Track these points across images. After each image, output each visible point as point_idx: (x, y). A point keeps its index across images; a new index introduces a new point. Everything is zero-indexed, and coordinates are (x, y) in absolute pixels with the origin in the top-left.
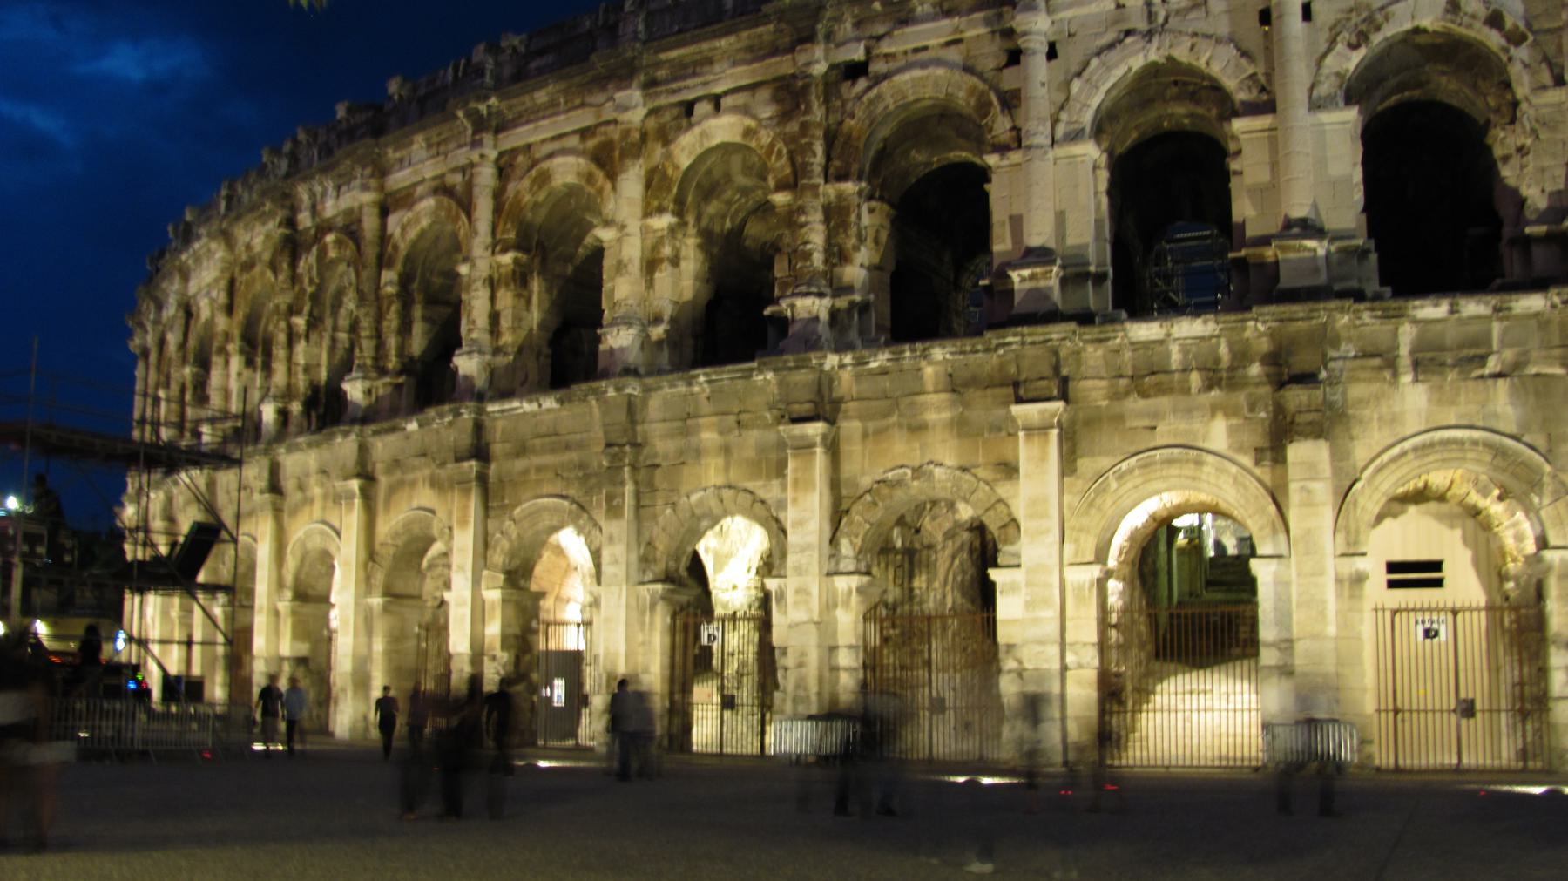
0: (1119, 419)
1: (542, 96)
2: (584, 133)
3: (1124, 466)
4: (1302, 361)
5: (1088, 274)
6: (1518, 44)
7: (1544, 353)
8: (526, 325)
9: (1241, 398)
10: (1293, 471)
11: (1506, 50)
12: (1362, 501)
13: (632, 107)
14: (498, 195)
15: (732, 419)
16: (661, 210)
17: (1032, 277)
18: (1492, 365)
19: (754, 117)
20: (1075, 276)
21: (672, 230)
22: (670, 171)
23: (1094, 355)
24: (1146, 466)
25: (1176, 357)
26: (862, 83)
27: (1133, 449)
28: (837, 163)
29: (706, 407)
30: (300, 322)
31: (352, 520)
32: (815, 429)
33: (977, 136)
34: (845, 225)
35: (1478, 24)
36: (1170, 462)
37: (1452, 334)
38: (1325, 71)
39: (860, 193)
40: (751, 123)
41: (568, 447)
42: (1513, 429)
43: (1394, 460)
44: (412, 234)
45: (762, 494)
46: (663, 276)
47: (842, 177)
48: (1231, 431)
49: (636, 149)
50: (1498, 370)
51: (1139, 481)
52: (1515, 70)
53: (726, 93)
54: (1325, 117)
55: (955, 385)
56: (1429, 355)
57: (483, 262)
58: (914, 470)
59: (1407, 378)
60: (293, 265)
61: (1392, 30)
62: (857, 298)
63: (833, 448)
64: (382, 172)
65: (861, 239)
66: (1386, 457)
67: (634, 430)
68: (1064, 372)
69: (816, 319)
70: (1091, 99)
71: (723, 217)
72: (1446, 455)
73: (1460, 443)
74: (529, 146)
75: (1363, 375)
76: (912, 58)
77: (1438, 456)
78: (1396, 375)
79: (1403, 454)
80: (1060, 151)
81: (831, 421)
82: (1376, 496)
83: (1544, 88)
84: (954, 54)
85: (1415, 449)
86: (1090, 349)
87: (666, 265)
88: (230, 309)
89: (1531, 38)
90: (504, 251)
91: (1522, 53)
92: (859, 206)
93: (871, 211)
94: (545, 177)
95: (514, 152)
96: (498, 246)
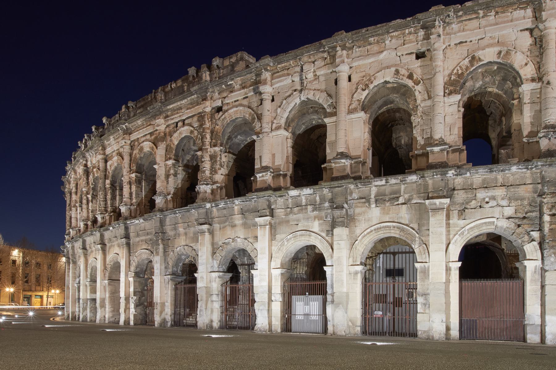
0: (288, 222)
1: (139, 122)
3: (289, 237)
4: (339, 200)
5: (280, 174)
6: (417, 85)
7: (418, 195)
8: (140, 196)
9: (323, 214)
10: (335, 238)
11: (414, 87)
12: (358, 247)
14: (131, 155)
16: (170, 159)
17: (263, 176)
18: (401, 200)
19: (193, 127)
20: (277, 175)
21: (174, 165)
23: (280, 201)
24: (295, 237)
25: (304, 202)
27: (292, 232)
28: (214, 141)
29: (180, 221)
33: (252, 131)
34: (216, 161)
35: (405, 78)
36: (302, 235)
37: (388, 189)
38: (354, 99)
39: (221, 151)
40: (192, 129)
42: (407, 222)
43: (368, 233)
44: (113, 168)
46: (171, 179)
47: (215, 146)
48: (320, 225)
49: (163, 138)
50: (403, 202)
51: (293, 242)
52: (417, 93)
54: (353, 116)
55: (243, 212)
56: (381, 197)
57: (128, 176)
58: (233, 239)
59: (373, 206)
62: (219, 185)
64: (104, 148)
66: (365, 233)
67: (162, 228)
68: (272, 207)
69: (206, 192)
70: (284, 115)
71: (193, 160)
72: (385, 231)
73: (388, 227)
75: (359, 205)
77: (382, 232)
78: (370, 205)
79: (372, 231)
80: (274, 133)
81: (210, 225)
82: (362, 246)
83: (425, 100)
85: (375, 230)
86: (279, 199)
87: (172, 176)
89: (422, 82)
91: (419, 88)
93: (226, 156)
94: (141, 149)
96: (131, 171)
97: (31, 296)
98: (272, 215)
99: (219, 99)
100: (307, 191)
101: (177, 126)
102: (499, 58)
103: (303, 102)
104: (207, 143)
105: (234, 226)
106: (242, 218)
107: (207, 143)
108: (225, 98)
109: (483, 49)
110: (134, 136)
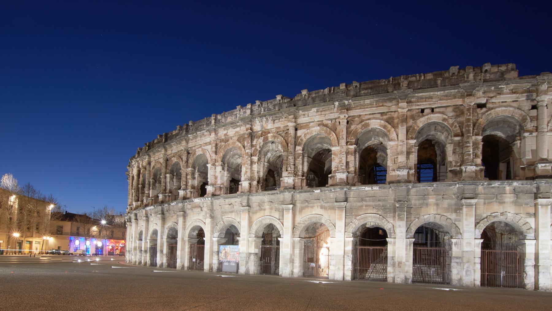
2: (382, 114)
13: (403, 108)
15: (441, 197)
22: (416, 128)
26: (484, 110)
28: (476, 131)
30: (255, 159)
31: (288, 217)
41: (379, 201)
45: (449, 217)
53: (436, 108)
60: (252, 142)
64: (296, 118)
74: (360, 115)
76: (501, 104)
84: (515, 104)
88: (216, 153)
90: (351, 145)
95: (354, 117)
97: (22, 241)
99: (484, 97)
106: (514, 197)
108: (491, 97)
110: (352, 113)
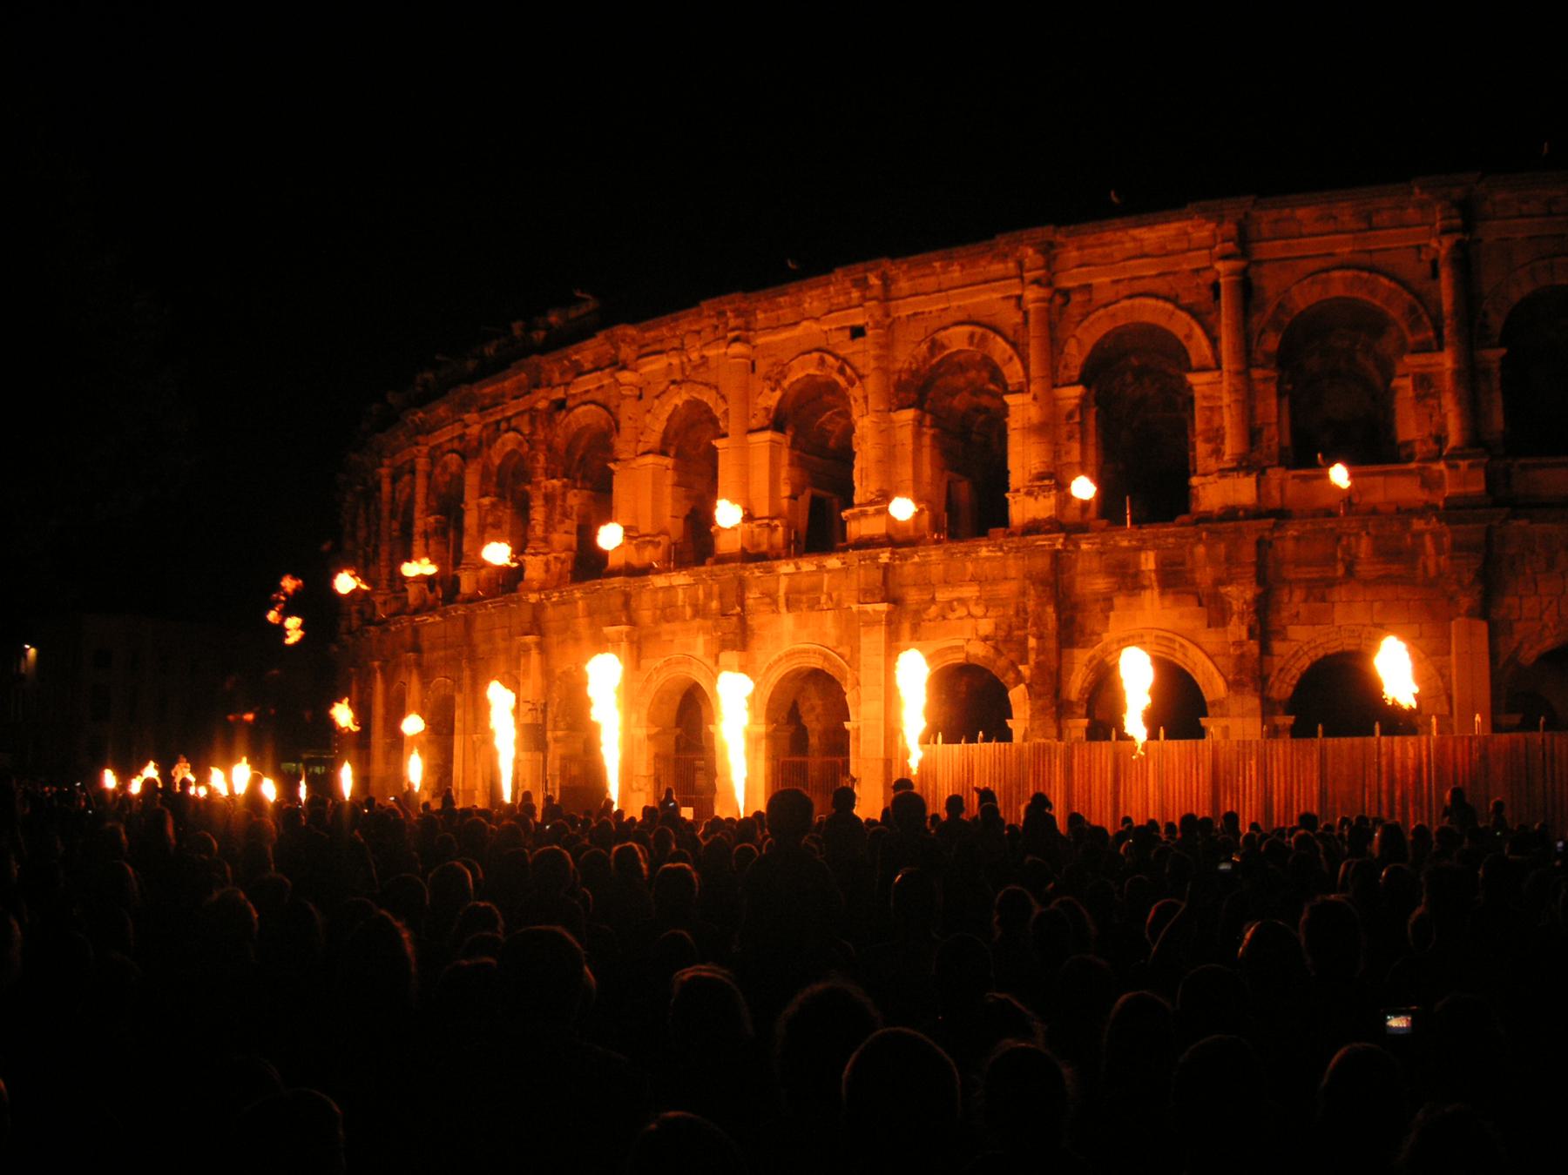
0: (658, 635)
21: (493, 505)
32: (530, 639)
37: (805, 583)
39: (565, 486)
48: (706, 643)
59: (783, 610)
61: (792, 378)
63: (542, 649)
65: (566, 515)
70: (656, 426)
79: (780, 659)
92: (564, 494)
98: (631, 622)
100: (681, 579)
101: (498, 429)
102: (971, 343)
103: (687, 402)
104: (540, 471)
105: (577, 639)
107: (540, 471)
109: (945, 328)
